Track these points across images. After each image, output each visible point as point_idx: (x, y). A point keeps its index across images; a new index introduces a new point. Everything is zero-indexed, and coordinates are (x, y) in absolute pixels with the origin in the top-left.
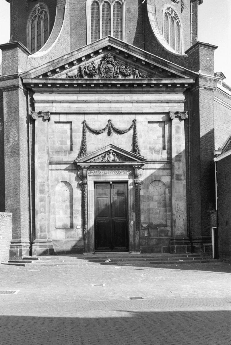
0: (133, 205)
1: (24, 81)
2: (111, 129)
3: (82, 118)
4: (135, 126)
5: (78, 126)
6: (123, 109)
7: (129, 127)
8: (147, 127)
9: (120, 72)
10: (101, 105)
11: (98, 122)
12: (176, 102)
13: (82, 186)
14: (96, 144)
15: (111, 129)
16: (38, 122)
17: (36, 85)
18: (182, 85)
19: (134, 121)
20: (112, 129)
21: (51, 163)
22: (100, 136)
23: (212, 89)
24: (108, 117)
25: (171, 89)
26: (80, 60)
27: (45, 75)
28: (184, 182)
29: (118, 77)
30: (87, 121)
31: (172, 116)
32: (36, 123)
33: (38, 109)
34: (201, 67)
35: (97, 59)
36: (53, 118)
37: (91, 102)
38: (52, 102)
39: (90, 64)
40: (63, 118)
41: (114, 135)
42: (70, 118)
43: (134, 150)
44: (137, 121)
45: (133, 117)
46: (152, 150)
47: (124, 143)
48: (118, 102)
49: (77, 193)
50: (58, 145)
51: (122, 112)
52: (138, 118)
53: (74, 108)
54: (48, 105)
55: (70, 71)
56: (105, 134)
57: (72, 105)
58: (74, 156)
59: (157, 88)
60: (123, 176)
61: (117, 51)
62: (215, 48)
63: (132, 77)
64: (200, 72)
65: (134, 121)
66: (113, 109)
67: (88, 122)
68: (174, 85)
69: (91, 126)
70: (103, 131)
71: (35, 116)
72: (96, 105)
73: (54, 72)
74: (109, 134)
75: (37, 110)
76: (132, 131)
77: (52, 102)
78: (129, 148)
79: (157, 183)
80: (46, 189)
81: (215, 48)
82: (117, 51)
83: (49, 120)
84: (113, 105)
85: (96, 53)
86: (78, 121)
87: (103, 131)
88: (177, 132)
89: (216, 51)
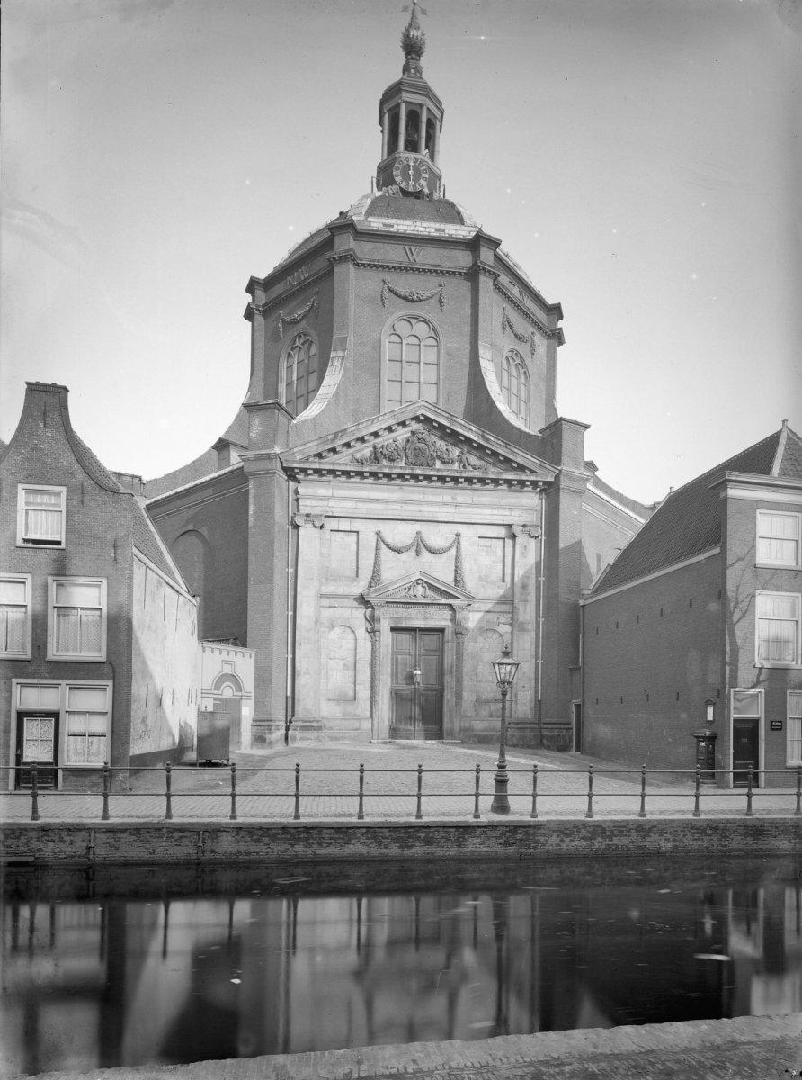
0: (452, 667)
2: (420, 545)
4: (459, 543)
5: (369, 538)
6: (439, 515)
7: (449, 544)
8: (475, 545)
9: (438, 457)
10: (405, 507)
11: (400, 534)
12: (527, 506)
13: (373, 632)
14: (396, 570)
15: (420, 545)
16: (307, 531)
17: (304, 471)
18: (534, 484)
20: (422, 546)
21: (322, 596)
22: (403, 556)
23: (580, 493)
24: (418, 527)
29: (435, 464)
30: (382, 530)
31: (517, 530)
32: (302, 531)
33: (305, 508)
34: (564, 459)
35: (401, 435)
36: (333, 524)
38: (329, 498)
39: (391, 441)
40: (344, 525)
41: (426, 555)
42: (357, 525)
43: (457, 581)
44: (462, 535)
47: (442, 570)
49: (365, 645)
51: (440, 520)
53: (362, 509)
55: (358, 451)
56: (413, 552)
57: (360, 505)
58: (359, 588)
60: (440, 619)
61: (434, 424)
62: (587, 427)
63: (456, 466)
64: (564, 468)
66: (426, 514)
68: (522, 483)
69: (389, 540)
70: (408, 548)
71: (299, 521)
72: (397, 506)
74: (418, 553)
75: (303, 510)
76: (453, 551)
77: (329, 498)
78: (448, 577)
79: (490, 634)
81: (587, 427)
82: (434, 424)
83: (322, 527)
84: (424, 508)
86: (368, 530)
87: (408, 548)
89: (587, 433)
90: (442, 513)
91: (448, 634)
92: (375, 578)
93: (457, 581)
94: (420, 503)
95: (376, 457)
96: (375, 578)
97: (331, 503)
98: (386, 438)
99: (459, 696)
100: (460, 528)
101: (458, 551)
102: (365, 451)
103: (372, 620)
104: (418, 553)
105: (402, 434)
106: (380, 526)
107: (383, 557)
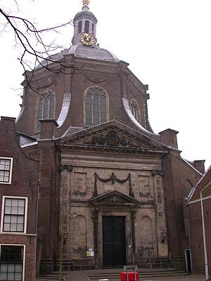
1: (57, 144)
3: (93, 170)
10: (107, 163)
11: (105, 174)
15: (113, 179)
19: (130, 175)
25: (153, 155)
26: (95, 133)
27: (71, 141)
28: (164, 217)
37: (101, 160)
38: (73, 159)
40: (80, 170)
41: (116, 183)
42: (86, 170)
45: (128, 172)
46: (141, 195)
48: (119, 162)
50: (76, 189)
52: (133, 173)
54: (71, 160)
58: (88, 197)
59: (145, 154)
63: (127, 146)
65: (130, 175)
67: (98, 173)
72: (103, 162)
73: (77, 139)
77: (73, 159)
80: (68, 220)
85: (105, 129)
86: (91, 173)
88: (158, 184)
90: (123, 165)
91: (128, 218)
92: (95, 193)
93: (132, 194)
94: (113, 161)
95: (93, 143)
96: (95, 193)
97: (75, 161)
98: (98, 135)
99: (134, 246)
100: (131, 173)
101: (130, 181)
102: (90, 139)
103: (96, 213)
104: (113, 183)
105: (105, 134)
106: (97, 171)
107: (97, 183)
